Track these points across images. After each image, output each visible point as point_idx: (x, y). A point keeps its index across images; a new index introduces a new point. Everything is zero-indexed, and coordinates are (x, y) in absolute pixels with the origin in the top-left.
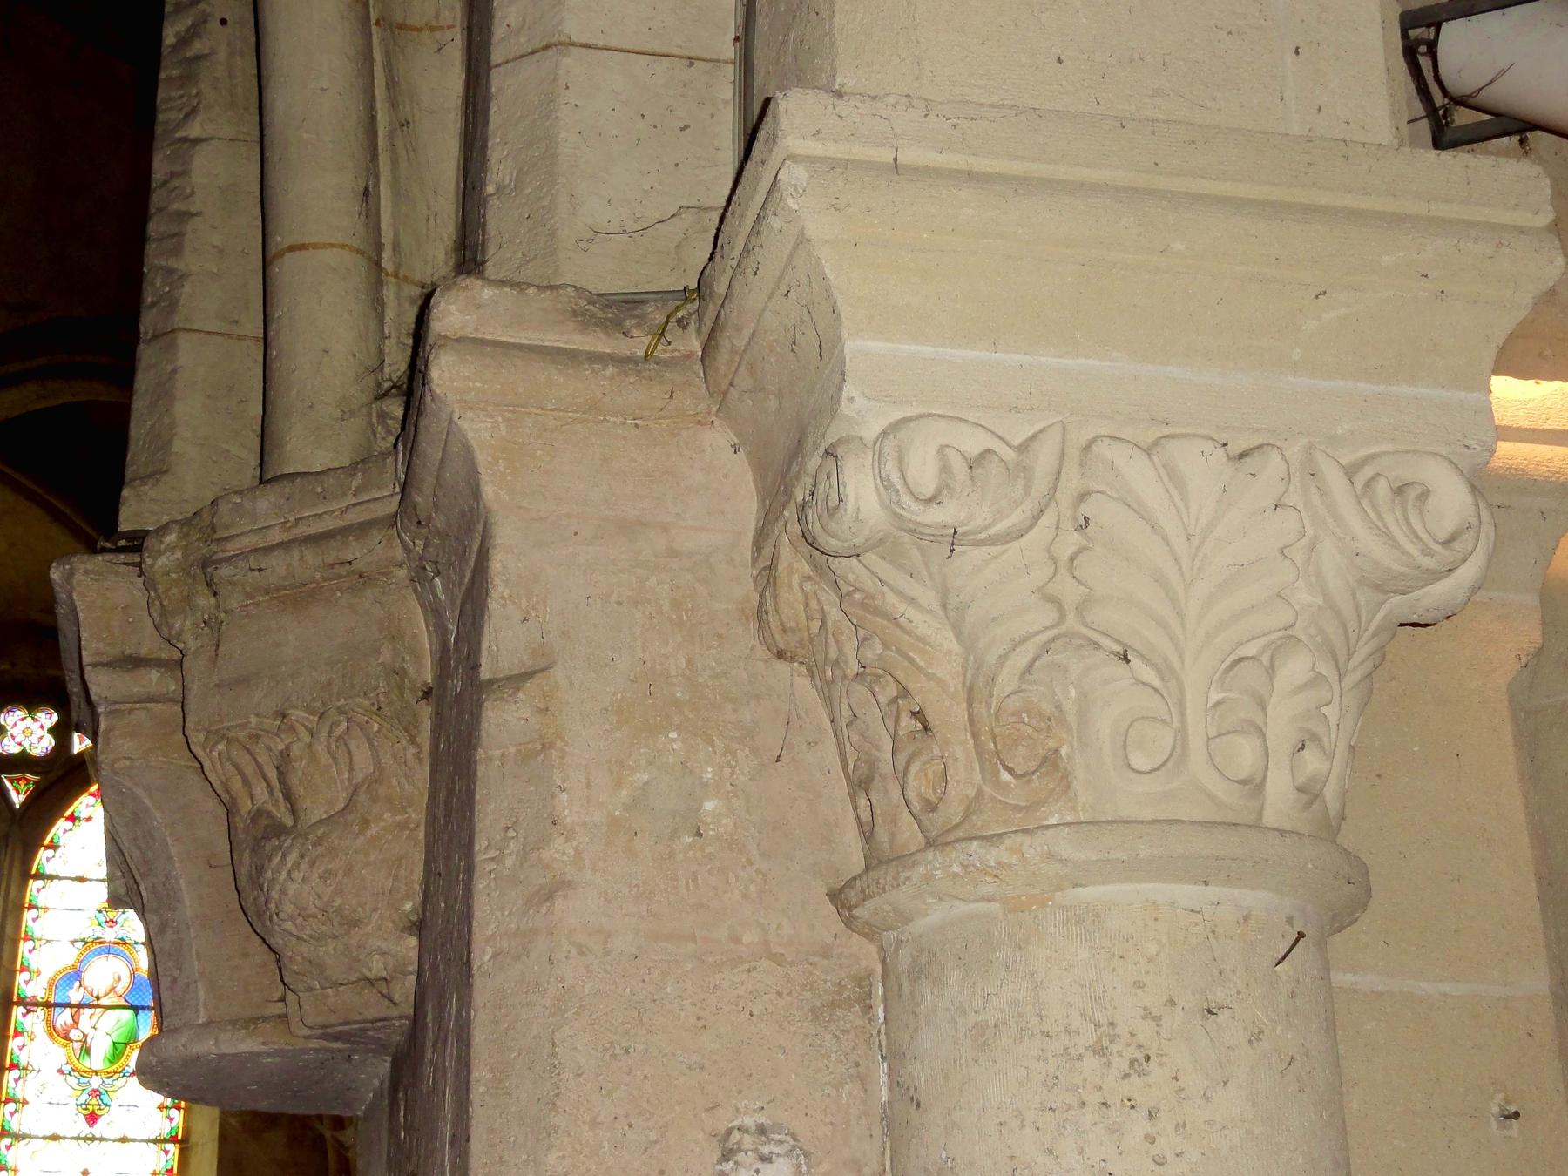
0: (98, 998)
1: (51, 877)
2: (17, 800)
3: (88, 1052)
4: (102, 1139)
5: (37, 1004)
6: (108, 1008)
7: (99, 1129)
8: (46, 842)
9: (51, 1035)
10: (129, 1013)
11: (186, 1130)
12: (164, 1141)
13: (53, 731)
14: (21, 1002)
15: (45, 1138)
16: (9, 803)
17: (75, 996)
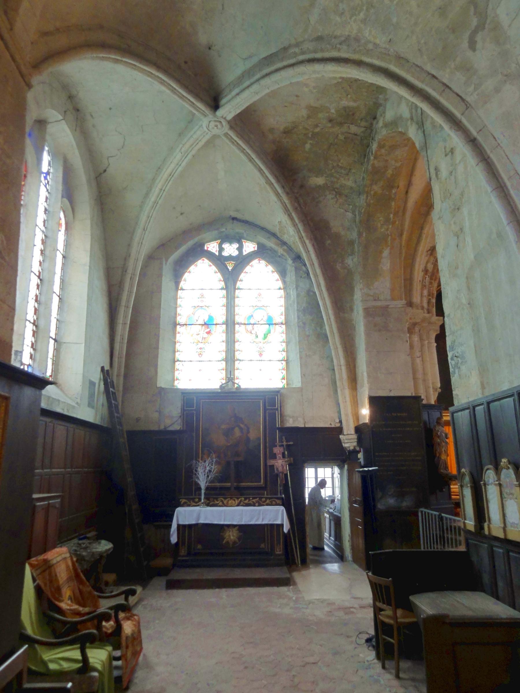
1: (242, 289)
2: (230, 268)
3: (257, 337)
7: (262, 358)
8: (239, 279)
10: (268, 326)
11: (287, 357)
12: (281, 361)
13: (238, 249)
14: (238, 324)
16: (228, 269)
17: (252, 322)
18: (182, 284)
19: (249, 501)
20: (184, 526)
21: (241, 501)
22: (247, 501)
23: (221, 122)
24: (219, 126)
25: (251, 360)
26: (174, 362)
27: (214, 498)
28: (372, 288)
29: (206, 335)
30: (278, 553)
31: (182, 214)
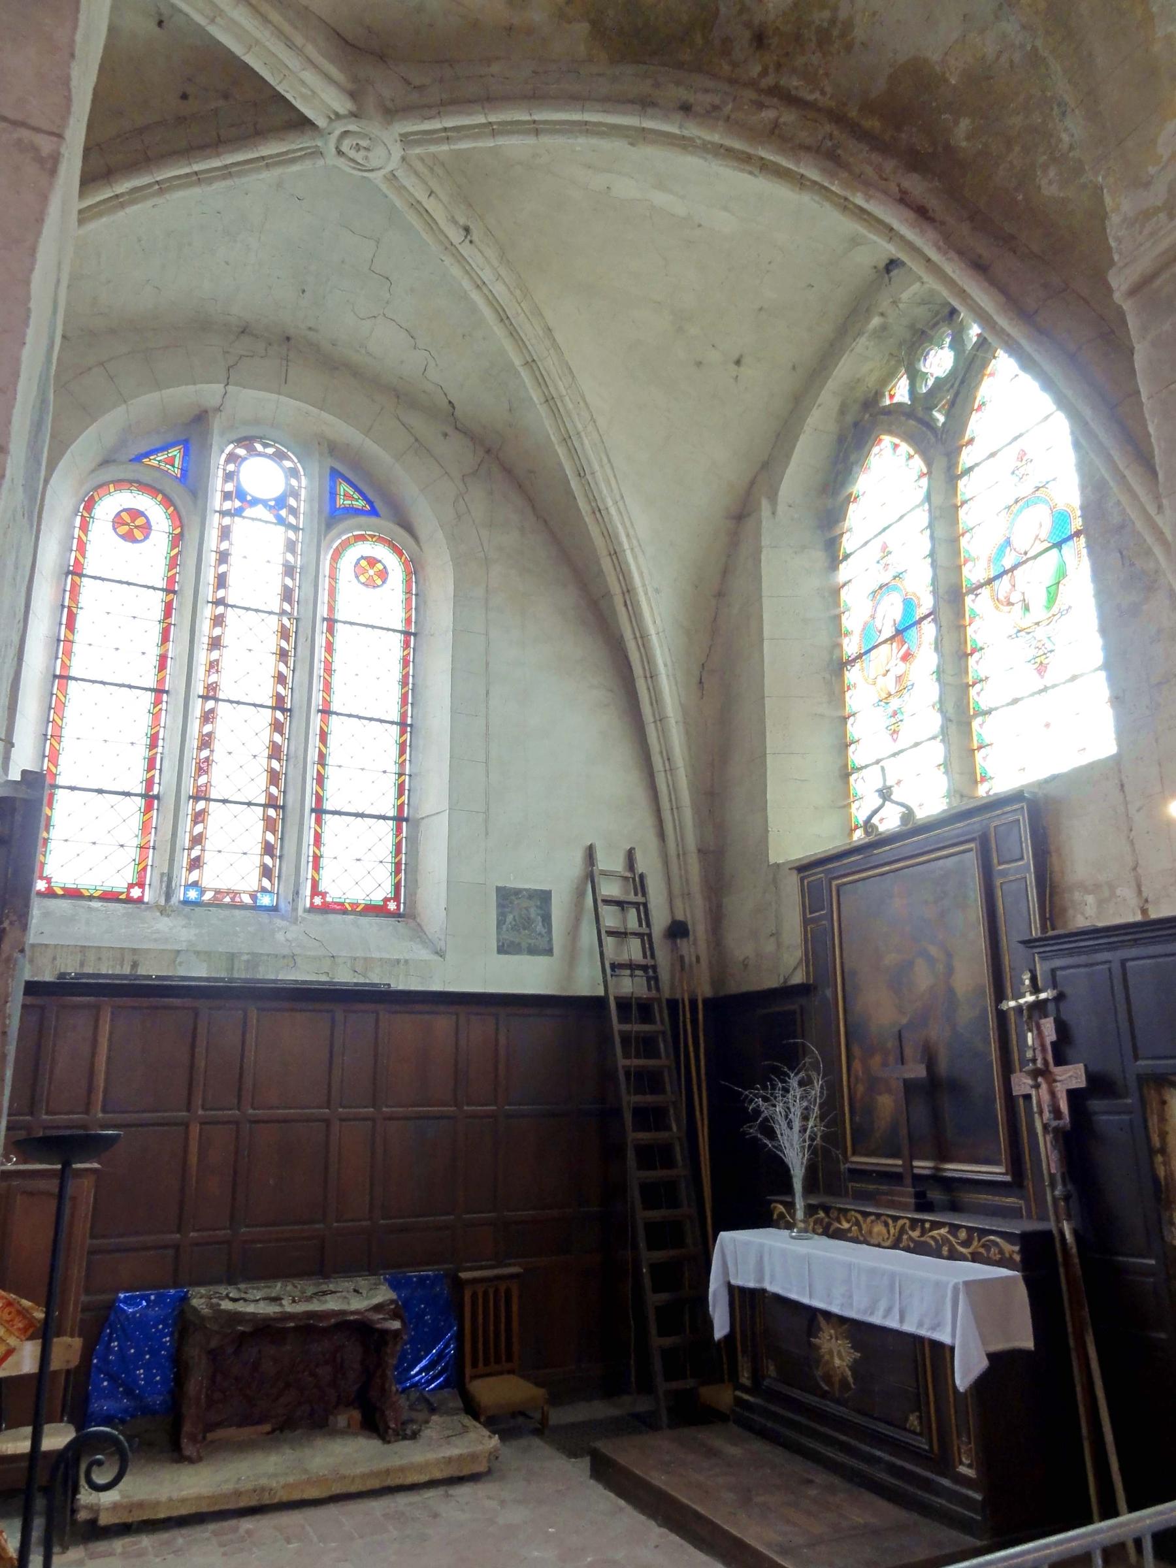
0: (1026, 553)
4: (1054, 686)
5: (981, 586)
6: (1035, 557)
9: (997, 608)
10: (1055, 551)
15: (1008, 704)
18: (848, 544)
19: (923, 1234)
20: (743, 1290)
21: (902, 1231)
22: (915, 1234)
23: (346, 132)
24: (364, 143)
25: (1015, 701)
26: (848, 775)
27: (840, 1210)
28: (1152, 170)
29: (902, 667)
30: (963, 1469)
31: (738, 362)
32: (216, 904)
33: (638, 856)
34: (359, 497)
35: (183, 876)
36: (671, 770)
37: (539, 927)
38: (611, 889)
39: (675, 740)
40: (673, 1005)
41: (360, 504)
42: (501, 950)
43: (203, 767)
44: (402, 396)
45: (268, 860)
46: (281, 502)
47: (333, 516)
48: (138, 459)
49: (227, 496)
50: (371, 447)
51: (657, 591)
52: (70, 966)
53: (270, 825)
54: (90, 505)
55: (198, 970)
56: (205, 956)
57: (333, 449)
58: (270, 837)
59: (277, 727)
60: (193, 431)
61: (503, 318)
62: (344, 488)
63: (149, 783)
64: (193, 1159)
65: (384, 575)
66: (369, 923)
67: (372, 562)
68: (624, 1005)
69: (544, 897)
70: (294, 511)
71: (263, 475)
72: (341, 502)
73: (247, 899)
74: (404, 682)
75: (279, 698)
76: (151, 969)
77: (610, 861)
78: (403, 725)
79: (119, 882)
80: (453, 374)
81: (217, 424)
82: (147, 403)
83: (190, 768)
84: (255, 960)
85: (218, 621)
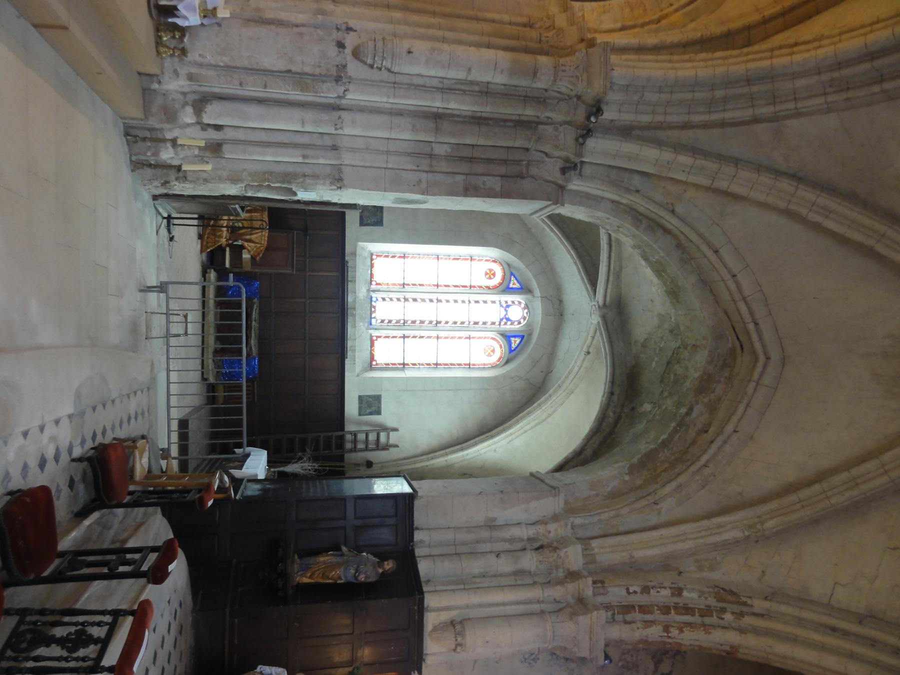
32: (372, 306)
33: (396, 449)
34: (516, 343)
35: (379, 295)
36: (428, 460)
37: (368, 411)
38: (383, 436)
39: (440, 461)
40: (341, 458)
41: (514, 346)
42: (360, 397)
43: (415, 300)
44: (552, 355)
45: (386, 321)
46: (508, 319)
47: (507, 336)
48: (512, 274)
49: (506, 302)
50: (531, 346)
51: (495, 451)
52: (350, 264)
53: (398, 322)
54: (494, 261)
55: (350, 299)
56: (355, 301)
57: (530, 335)
58: (394, 322)
59: (431, 322)
60: (524, 289)
61: (569, 373)
62: (518, 340)
63: (408, 285)
64: (296, 300)
65: (489, 355)
66: (367, 355)
67: (493, 351)
68: (342, 438)
69: (378, 412)
70: (506, 324)
71: (517, 313)
72: (513, 339)
73: (373, 315)
74: (452, 364)
75: (439, 322)
76: (350, 286)
77: (394, 438)
78: (437, 364)
79: (377, 278)
80: (560, 368)
81: (529, 296)
82: (529, 274)
83: (414, 296)
84: (354, 316)
85: (463, 302)
